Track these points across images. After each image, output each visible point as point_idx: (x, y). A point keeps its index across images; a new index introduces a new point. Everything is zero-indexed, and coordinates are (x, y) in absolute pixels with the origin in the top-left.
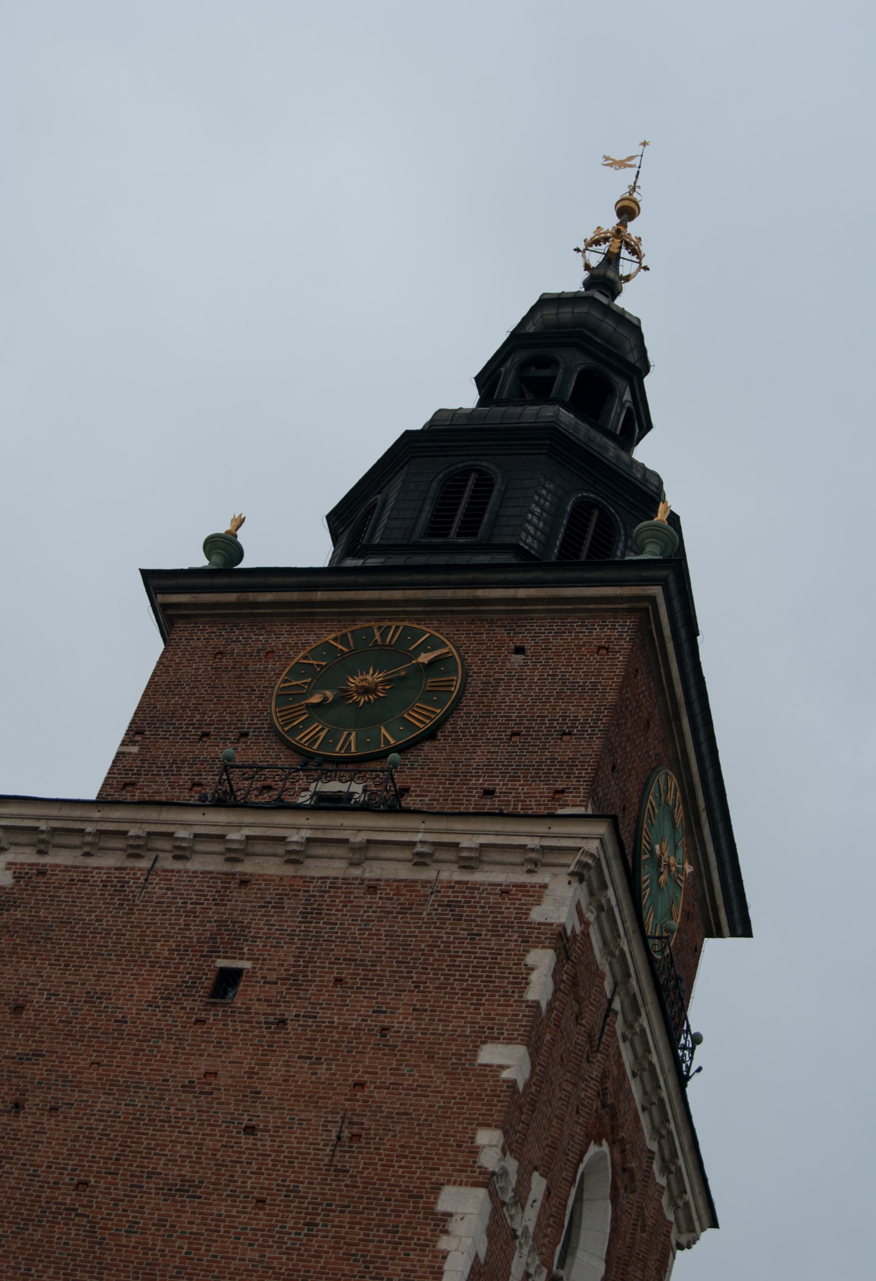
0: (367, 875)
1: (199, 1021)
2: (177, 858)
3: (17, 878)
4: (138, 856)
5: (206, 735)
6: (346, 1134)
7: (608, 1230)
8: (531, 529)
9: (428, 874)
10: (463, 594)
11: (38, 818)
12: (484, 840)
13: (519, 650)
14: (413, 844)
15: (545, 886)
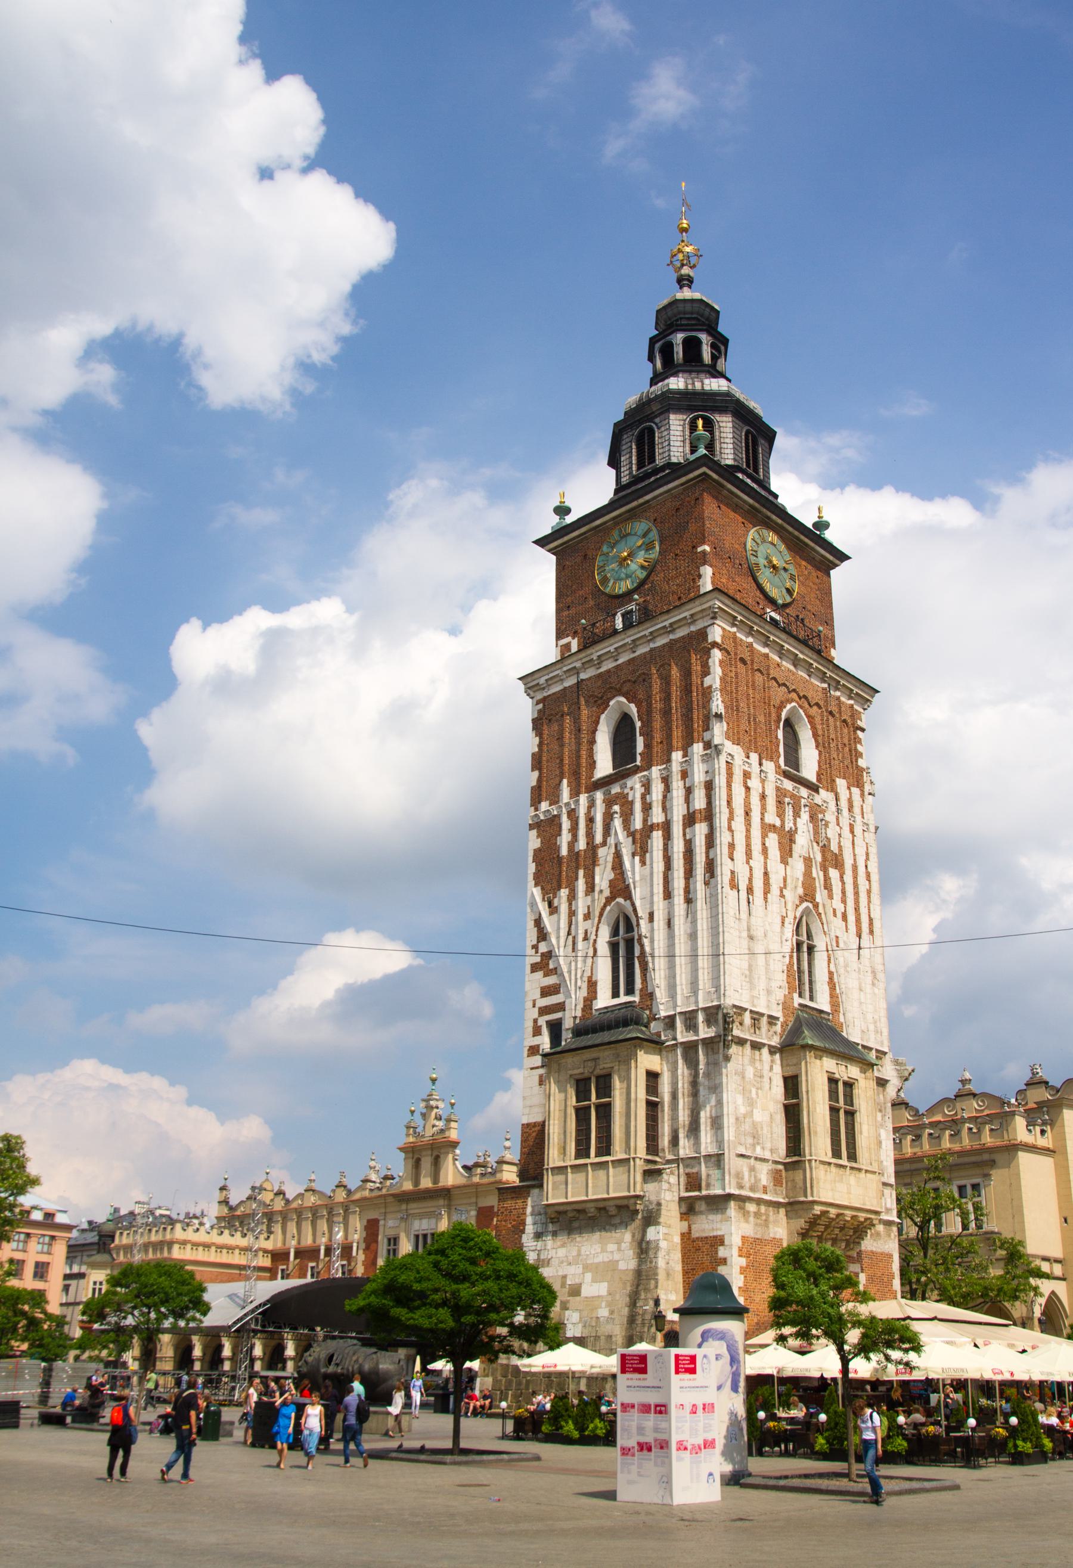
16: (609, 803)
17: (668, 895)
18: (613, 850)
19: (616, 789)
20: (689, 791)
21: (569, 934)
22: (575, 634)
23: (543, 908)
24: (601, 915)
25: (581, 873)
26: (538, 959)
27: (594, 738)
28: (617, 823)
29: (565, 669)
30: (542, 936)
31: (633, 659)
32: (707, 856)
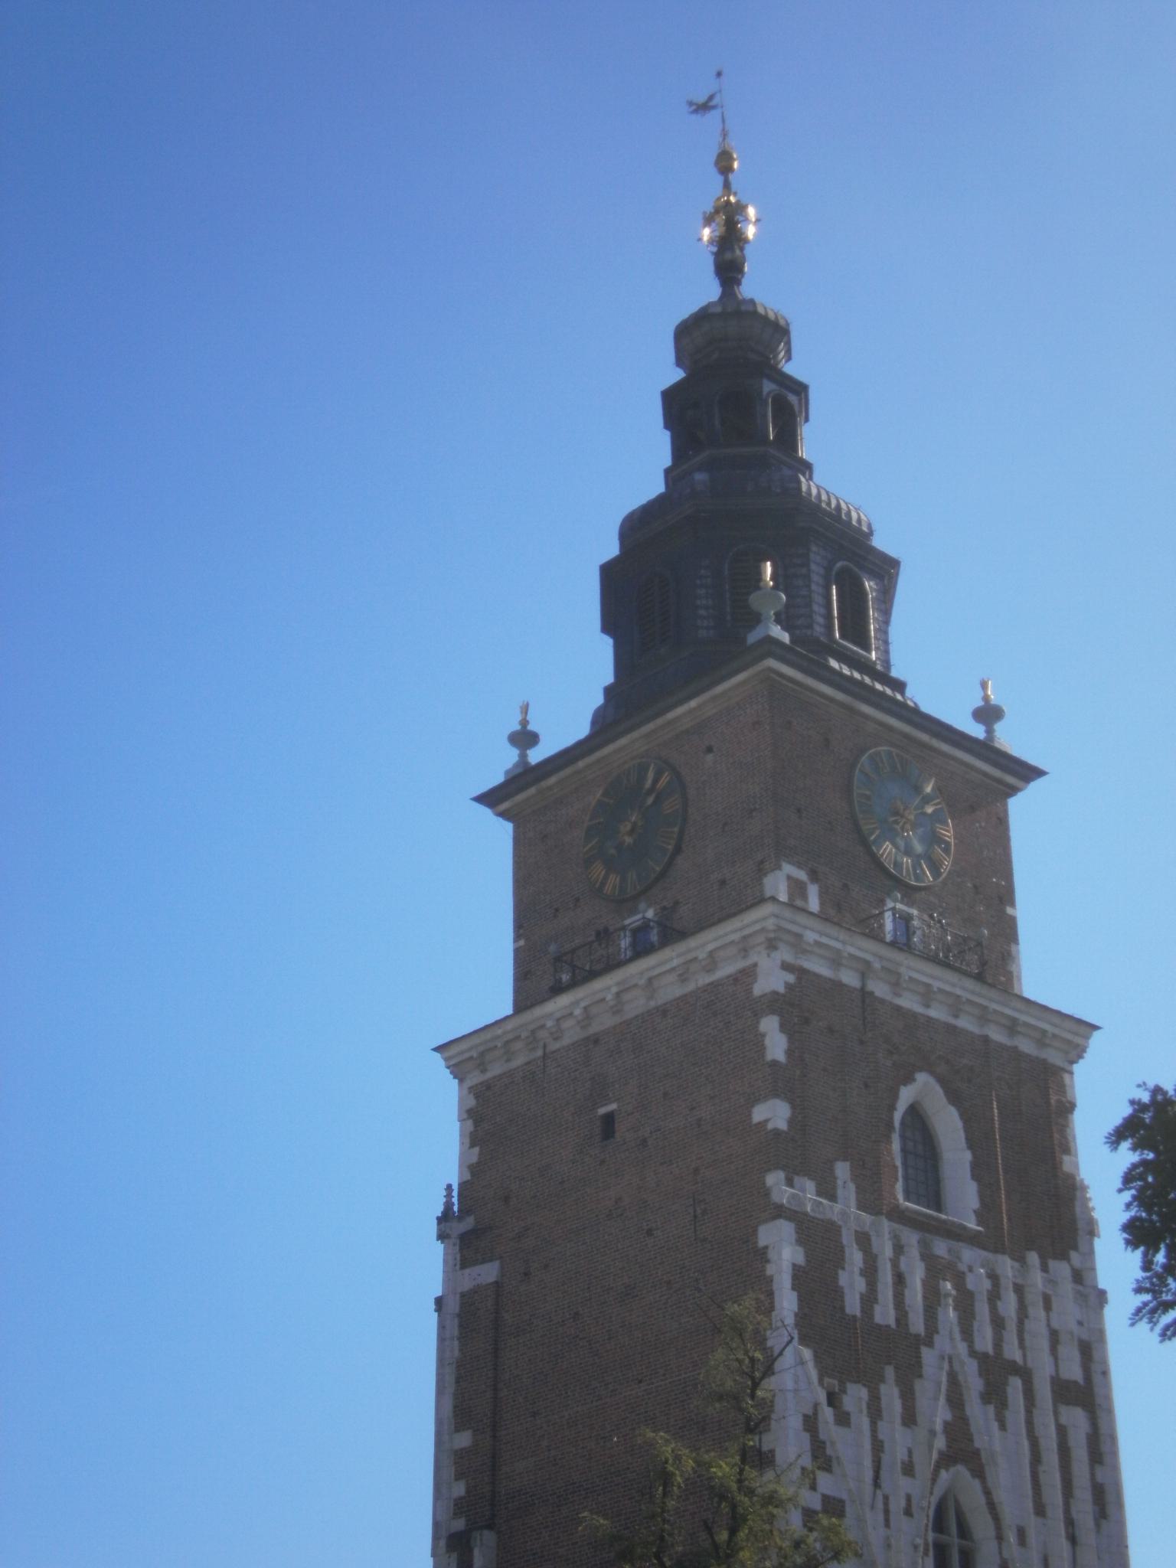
0: (660, 1002)
1: (603, 1162)
2: (556, 1039)
3: (477, 1097)
4: (534, 1049)
5: (557, 910)
6: (699, 1211)
7: (959, 1124)
8: (702, 612)
9: (691, 987)
10: (660, 721)
11: (470, 1049)
12: (710, 947)
13: (710, 750)
14: (673, 969)
15: (755, 965)
16: (935, 1270)
17: (1040, 1510)
18: (946, 1366)
19: (941, 1248)
20: (1054, 1337)
21: (876, 1482)
22: (814, 876)
23: (822, 1397)
24: (934, 1480)
25: (890, 1372)
26: (818, 1506)
27: (891, 1118)
28: (949, 1314)
29: (852, 950)
30: (822, 1457)
31: (955, 1027)
32: (1093, 1475)
